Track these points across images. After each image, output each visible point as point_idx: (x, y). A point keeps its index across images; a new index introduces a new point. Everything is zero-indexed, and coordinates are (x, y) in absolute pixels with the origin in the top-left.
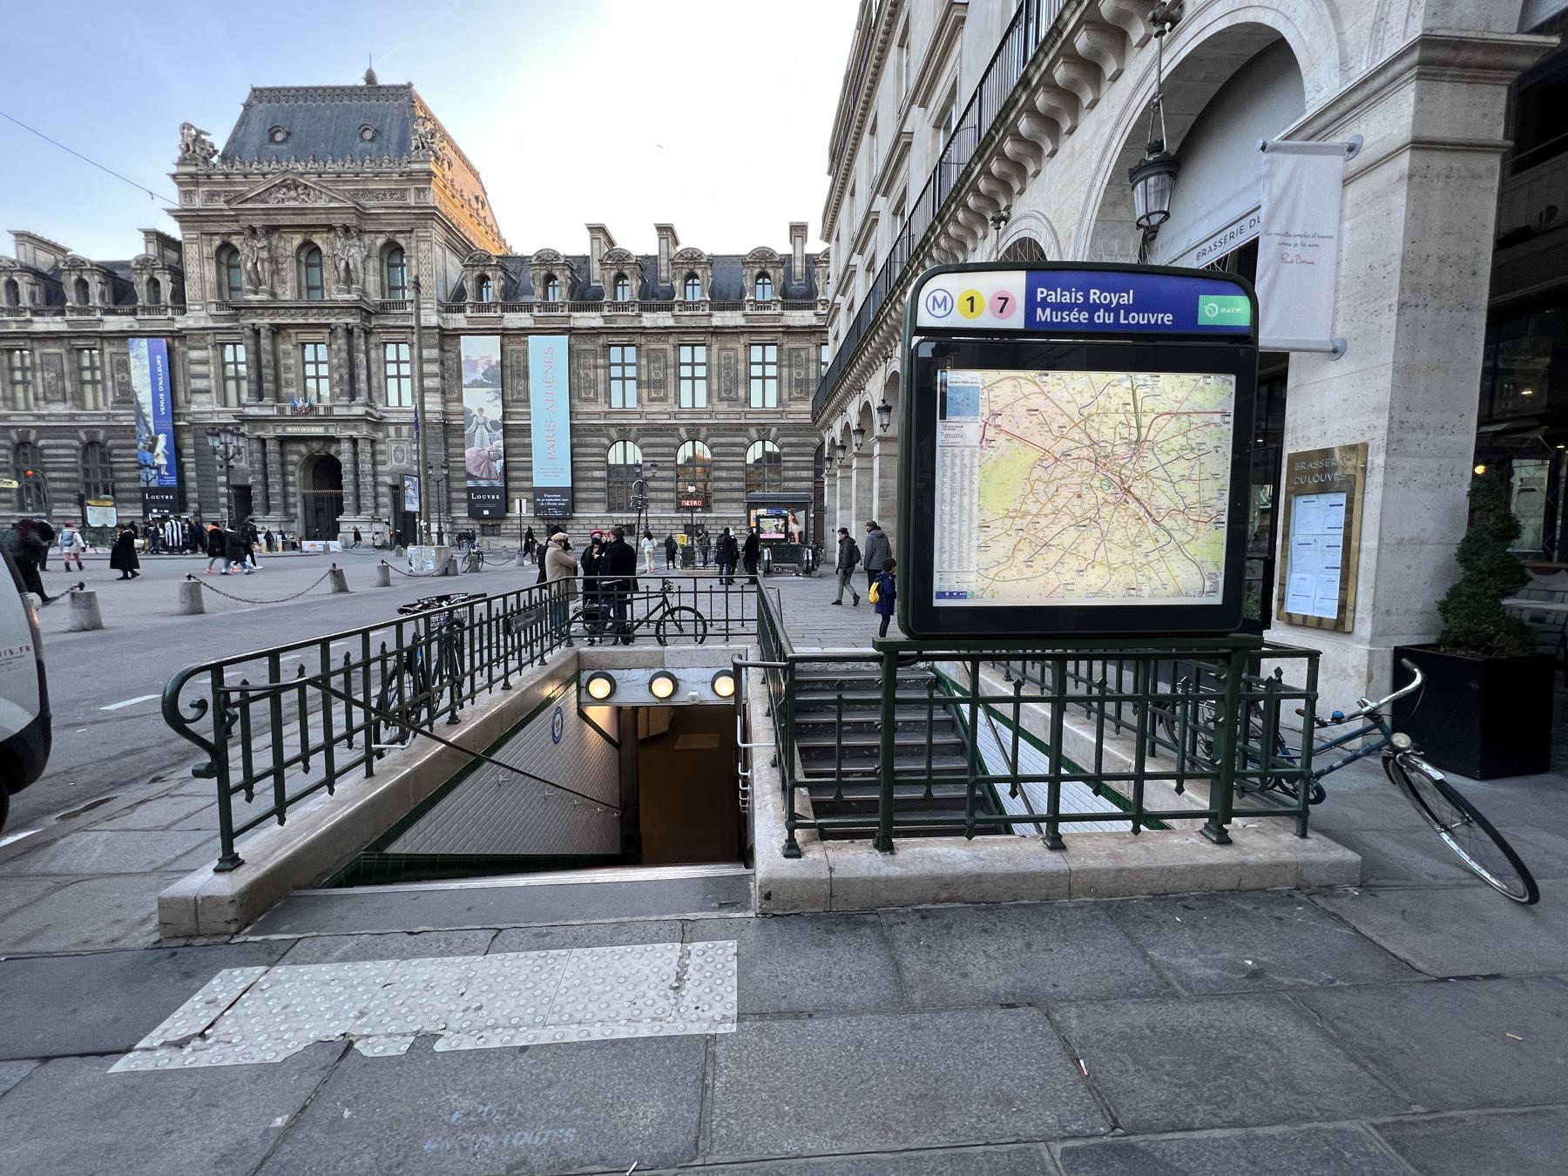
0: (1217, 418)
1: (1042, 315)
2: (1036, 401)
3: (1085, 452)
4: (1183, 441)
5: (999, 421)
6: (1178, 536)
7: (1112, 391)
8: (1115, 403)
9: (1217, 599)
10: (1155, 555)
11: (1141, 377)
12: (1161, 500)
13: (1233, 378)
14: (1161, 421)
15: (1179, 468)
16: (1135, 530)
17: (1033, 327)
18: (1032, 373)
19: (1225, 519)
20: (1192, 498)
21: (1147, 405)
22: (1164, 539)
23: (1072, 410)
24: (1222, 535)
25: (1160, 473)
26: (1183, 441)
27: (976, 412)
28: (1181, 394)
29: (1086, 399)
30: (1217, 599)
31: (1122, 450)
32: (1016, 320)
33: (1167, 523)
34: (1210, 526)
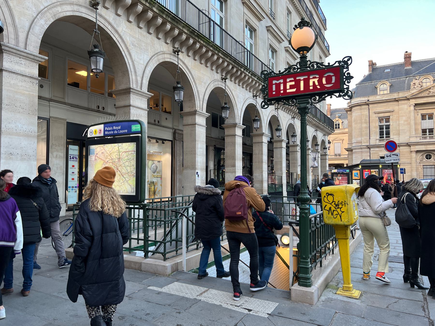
0: (133, 152)
1: (106, 133)
2: (103, 151)
3: (111, 161)
4: (127, 158)
5: (97, 155)
6: (127, 179)
7: (115, 148)
8: (116, 150)
9: (134, 194)
10: (123, 183)
11: (120, 144)
12: (123, 171)
13: (135, 143)
14: (123, 154)
15: (127, 164)
16: (119, 178)
17: (105, 135)
18: (102, 145)
19: (135, 175)
20: (129, 170)
21: (121, 150)
22: (124, 180)
23: (108, 152)
24: (135, 179)
25: (123, 165)
26: (127, 158)
27: (94, 154)
28: (126, 147)
29: (110, 150)
30: (134, 194)
31: (117, 160)
32: (102, 135)
33: (125, 176)
34: (133, 177)
